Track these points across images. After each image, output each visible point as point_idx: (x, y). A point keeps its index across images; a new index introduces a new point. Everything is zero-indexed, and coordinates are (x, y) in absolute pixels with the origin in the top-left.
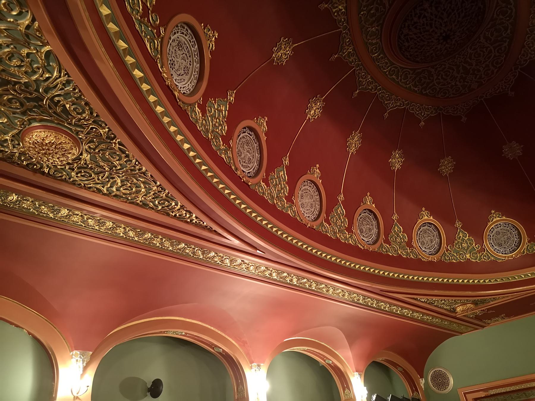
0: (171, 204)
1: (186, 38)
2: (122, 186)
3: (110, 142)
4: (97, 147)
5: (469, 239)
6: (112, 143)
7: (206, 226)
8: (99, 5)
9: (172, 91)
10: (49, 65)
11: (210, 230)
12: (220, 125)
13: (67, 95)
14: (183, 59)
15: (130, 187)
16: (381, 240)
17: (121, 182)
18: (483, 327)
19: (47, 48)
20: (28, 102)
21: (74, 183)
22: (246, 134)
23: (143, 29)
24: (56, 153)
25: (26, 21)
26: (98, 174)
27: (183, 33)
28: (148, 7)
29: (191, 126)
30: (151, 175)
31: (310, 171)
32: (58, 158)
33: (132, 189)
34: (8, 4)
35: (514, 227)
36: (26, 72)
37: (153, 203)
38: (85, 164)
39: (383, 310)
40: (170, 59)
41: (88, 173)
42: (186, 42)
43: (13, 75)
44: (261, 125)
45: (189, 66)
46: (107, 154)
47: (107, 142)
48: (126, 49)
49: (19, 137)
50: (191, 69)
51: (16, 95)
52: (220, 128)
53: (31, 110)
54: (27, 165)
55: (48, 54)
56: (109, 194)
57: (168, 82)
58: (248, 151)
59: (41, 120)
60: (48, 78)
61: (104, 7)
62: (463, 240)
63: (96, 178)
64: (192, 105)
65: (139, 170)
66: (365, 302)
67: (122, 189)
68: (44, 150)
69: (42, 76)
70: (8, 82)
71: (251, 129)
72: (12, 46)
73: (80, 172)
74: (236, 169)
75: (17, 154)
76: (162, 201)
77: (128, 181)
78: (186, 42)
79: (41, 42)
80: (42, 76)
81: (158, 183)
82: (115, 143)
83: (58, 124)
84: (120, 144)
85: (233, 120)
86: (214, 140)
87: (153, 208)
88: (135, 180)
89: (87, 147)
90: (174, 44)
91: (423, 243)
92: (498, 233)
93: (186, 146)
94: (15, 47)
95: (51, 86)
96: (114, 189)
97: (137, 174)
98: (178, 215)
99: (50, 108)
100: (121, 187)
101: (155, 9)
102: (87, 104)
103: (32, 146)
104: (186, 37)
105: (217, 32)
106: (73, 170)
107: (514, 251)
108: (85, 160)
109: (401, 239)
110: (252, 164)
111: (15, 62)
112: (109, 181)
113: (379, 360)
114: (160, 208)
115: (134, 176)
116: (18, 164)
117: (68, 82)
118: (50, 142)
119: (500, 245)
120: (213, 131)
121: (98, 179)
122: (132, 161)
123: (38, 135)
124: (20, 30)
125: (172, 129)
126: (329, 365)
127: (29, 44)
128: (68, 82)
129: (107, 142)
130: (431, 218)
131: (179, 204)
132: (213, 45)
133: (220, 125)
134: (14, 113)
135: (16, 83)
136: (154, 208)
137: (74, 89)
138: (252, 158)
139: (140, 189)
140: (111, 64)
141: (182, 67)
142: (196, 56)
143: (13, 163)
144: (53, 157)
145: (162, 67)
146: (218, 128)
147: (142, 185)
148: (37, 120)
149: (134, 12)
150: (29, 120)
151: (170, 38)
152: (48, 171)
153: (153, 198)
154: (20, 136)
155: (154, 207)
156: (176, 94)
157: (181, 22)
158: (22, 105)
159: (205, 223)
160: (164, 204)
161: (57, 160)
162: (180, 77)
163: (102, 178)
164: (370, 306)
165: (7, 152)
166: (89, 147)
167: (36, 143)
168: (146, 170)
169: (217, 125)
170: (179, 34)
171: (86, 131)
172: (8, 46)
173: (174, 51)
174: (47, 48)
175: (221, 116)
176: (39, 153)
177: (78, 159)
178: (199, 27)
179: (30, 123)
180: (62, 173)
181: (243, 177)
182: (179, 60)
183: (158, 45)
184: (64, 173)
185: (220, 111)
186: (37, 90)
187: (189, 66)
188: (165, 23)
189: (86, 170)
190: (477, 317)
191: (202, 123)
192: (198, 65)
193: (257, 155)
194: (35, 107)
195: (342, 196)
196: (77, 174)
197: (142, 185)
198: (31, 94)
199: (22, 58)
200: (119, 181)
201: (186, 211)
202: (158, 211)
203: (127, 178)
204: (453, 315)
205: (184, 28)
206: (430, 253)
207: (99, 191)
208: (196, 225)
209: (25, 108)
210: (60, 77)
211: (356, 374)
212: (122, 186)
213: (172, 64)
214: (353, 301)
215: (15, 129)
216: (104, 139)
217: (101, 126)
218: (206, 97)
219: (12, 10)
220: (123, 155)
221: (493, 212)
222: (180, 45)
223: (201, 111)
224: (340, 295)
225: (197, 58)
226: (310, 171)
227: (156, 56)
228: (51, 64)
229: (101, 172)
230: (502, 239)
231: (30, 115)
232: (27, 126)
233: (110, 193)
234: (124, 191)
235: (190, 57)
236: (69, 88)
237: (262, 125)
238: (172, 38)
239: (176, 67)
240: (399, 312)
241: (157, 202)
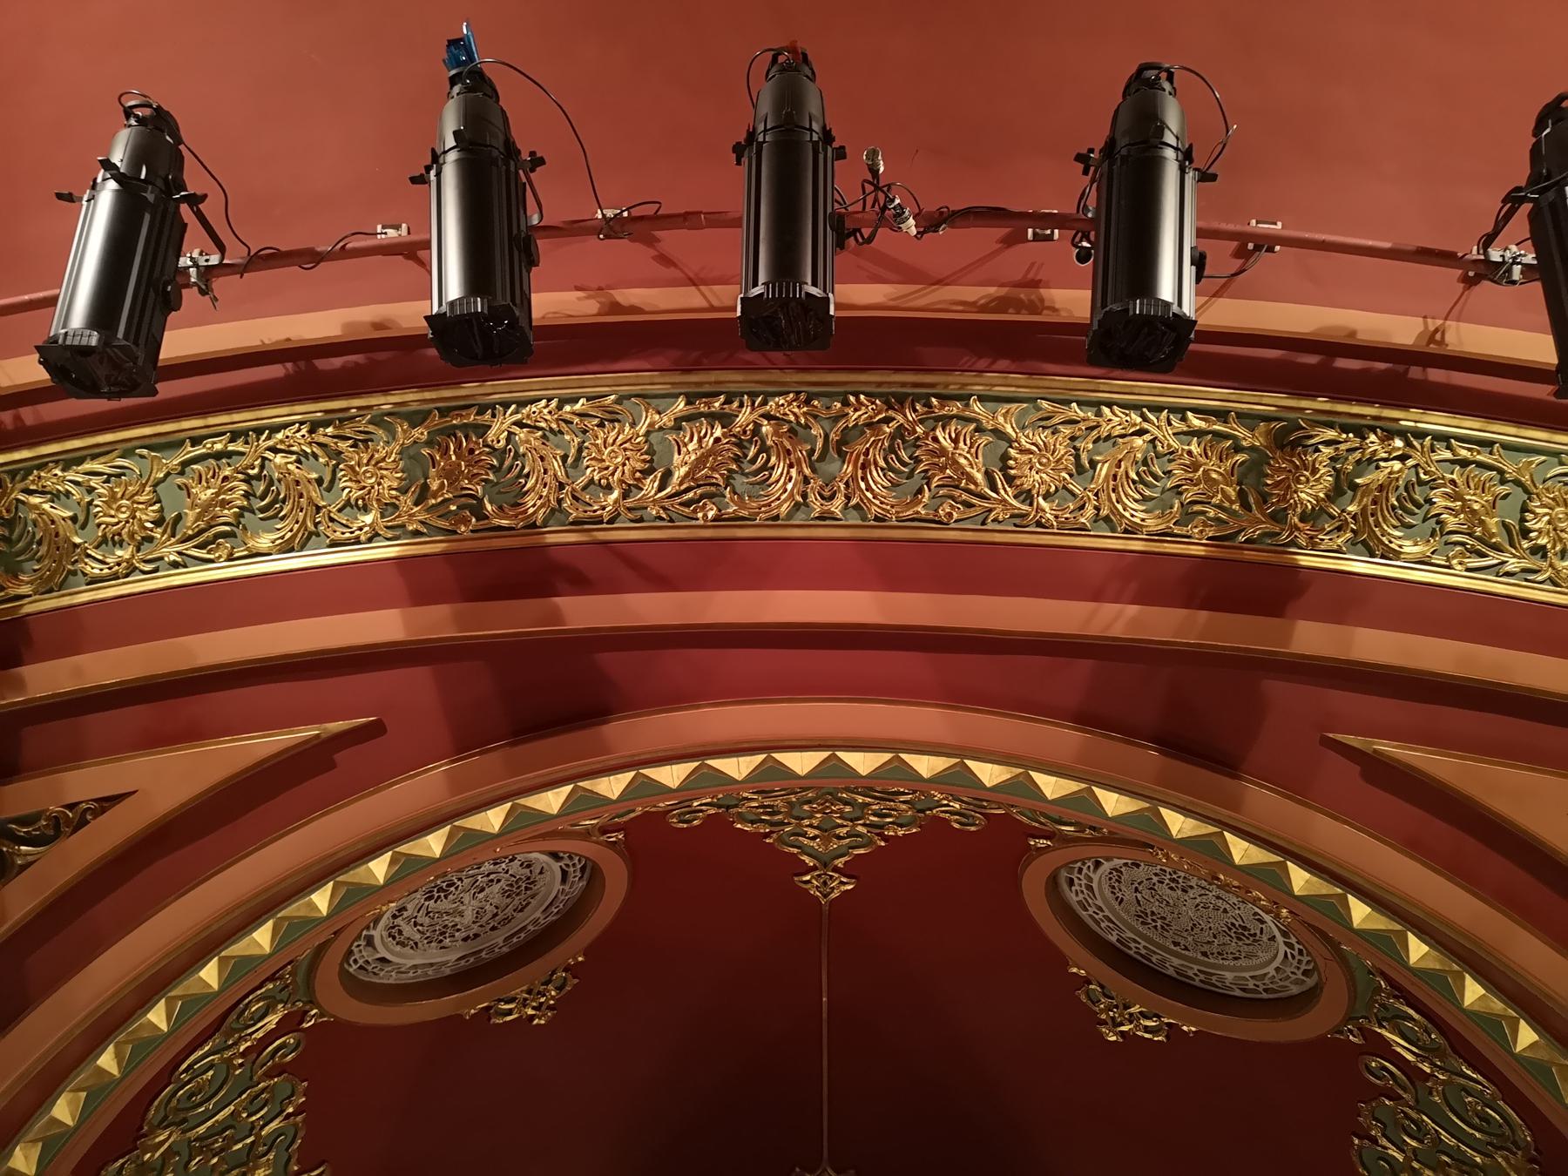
8: (31, 1136)
61: (36, 1151)
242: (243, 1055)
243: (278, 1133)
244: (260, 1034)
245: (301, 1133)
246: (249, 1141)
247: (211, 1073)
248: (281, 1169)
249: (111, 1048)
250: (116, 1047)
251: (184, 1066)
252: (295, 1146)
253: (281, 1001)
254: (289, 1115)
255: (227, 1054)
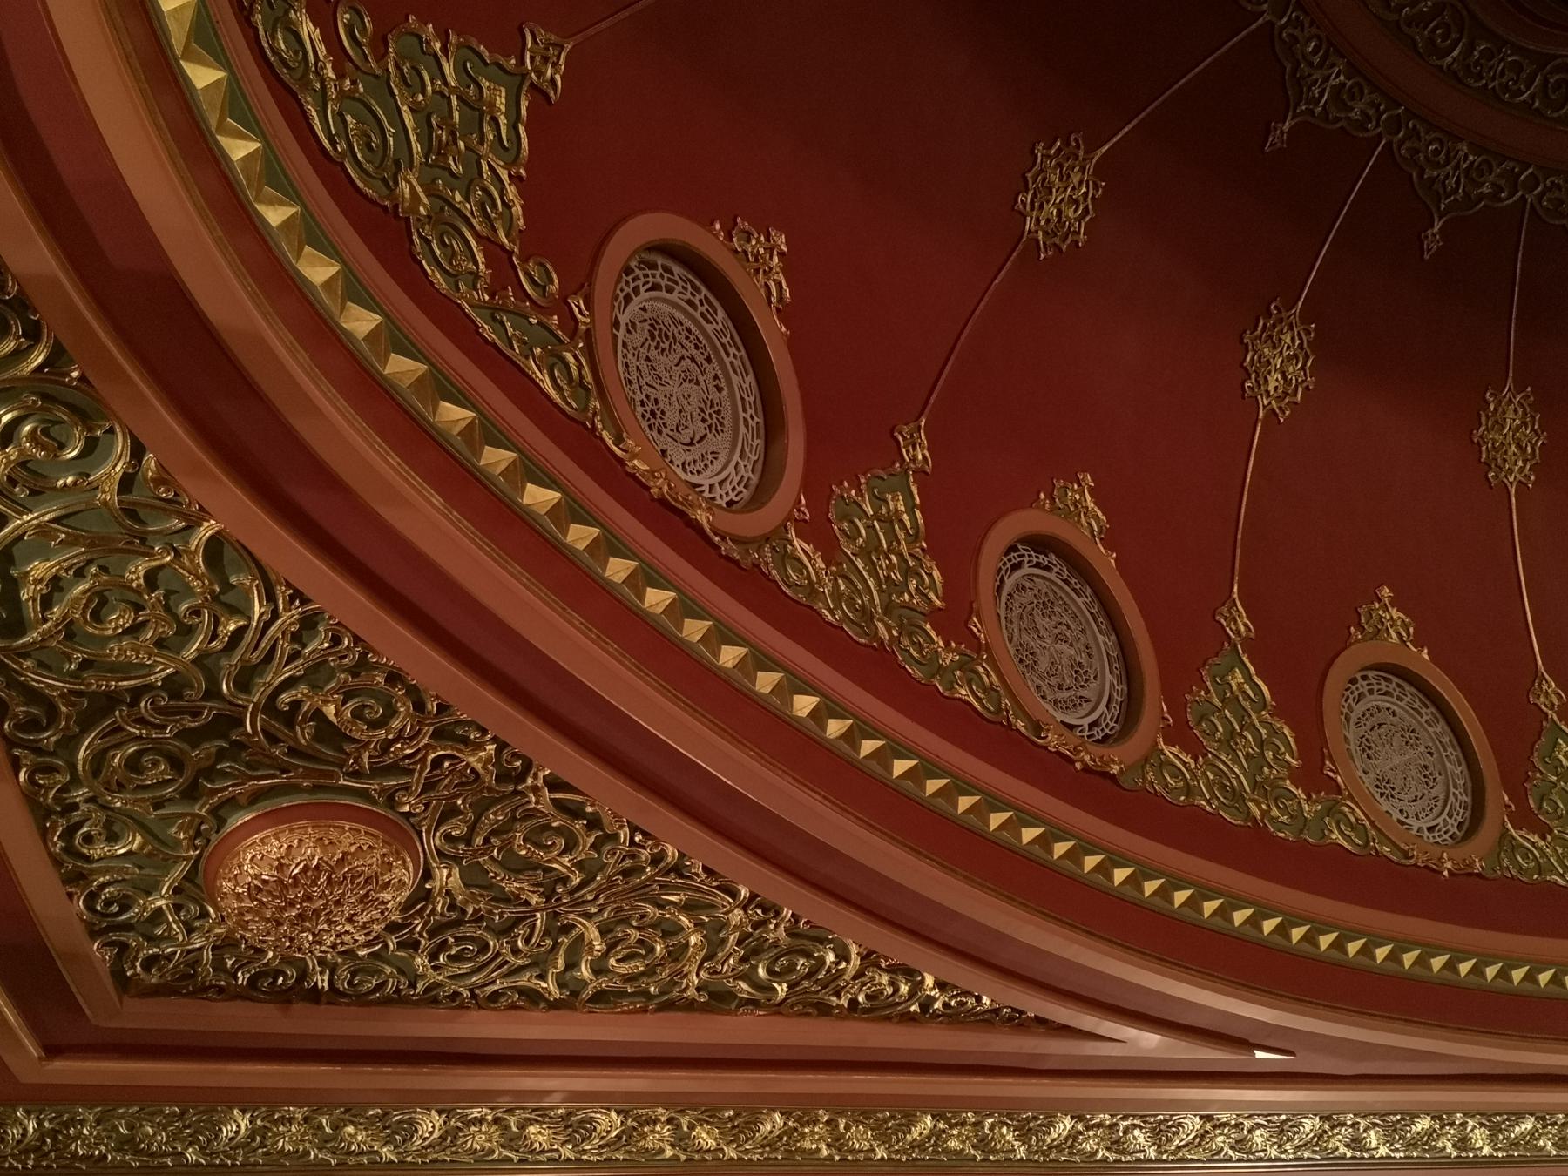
0: (822, 961)
1: (671, 300)
2: (611, 947)
3: (516, 793)
4: (473, 828)
6: (523, 794)
7: (996, 1011)
8: (335, 311)
9: (682, 515)
10: (227, 587)
11: (1019, 1022)
12: (908, 572)
13: (316, 674)
14: (686, 378)
15: (640, 942)
17: (604, 932)
19: (207, 530)
20: (194, 748)
21: (431, 998)
22: (1026, 570)
23: (510, 331)
24: (338, 903)
25: (115, 467)
26: (506, 931)
27: (655, 287)
28: (502, 247)
29: (797, 619)
30: (705, 869)
31: (1360, 626)
32: (350, 920)
33: (653, 950)
34: (45, 432)
36: (160, 643)
37: (749, 977)
38: (452, 907)
40: (640, 397)
41: (473, 939)
42: (678, 315)
43: (124, 670)
44: (1072, 514)
45: (715, 396)
46: (519, 841)
47: (504, 797)
48: (471, 425)
49: (196, 889)
50: (727, 403)
51: (148, 737)
52: (913, 584)
53: (210, 773)
54: (253, 981)
55: (214, 548)
56: (572, 999)
57: (659, 487)
58: (1058, 638)
59: (256, 797)
60: (239, 633)
61: (354, 309)
63: (507, 950)
64: (775, 536)
65: (656, 860)
67: (612, 961)
68: (291, 904)
69: (214, 637)
70: (111, 700)
71: (1040, 543)
72: (93, 570)
73: (444, 946)
74: (1037, 728)
75: (207, 955)
76: (783, 961)
77: (626, 921)
78: (678, 315)
79: (182, 516)
80: (214, 637)
81: (744, 892)
82: (535, 789)
83: (317, 788)
84: (554, 784)
85: (952, 539)
86: (905, 642)
87: (753, 1002)
88: (651, 910)
89: (438, 840)
90: (636, 339)
93: (804, 705)
94: (104, 569)
95: (256, 657)
96: (585, 972)
97: (651, 879)
98: (861, 998)
99: (273, 739)
100: (606, 955)
101: (535, 241)
102: (393, 678)
103: (247, 904)
104: (674, 297)
105: (780, 229)
106: (415, 945)
108: (448, 893)
110: (1094, 685)
111: (118, 619)
112: (556, 945)
114: (782, 990)
115: (642, 893)
116: (221, 990)
117: (309, 623)
118: (306, 868)
120: (888, 609)
121: (516, 952)
122: (615, 837)
123: (262, 853)
124: (105, 503)
125: (729, 656)
127: (143, 541)
128: (309, 623)
129: (504, 797)
131: (854, 949)
132: (779, 284)
133: (908, 572)
134: (158, 805)
135: (137, 693)
136: (762, 1001)
137: (336, 641)
138: (1084, 659)
139: (681, 938)
140: (437, 500)
141: (693, 408)
142: (732, 350)
143: (202, 991)
144: (330, 922)
145: (618, 440)
146: (902, 588)
147: (684, 921)
148: (243, 800)
149: (462, 285)
150: (214, 811)
151: (616, 324)
152: (331, 982)
153: (743, 960)
154: (200, 880)
155: (760, 996)
156: (702, 517)
157: (635, 252)
158: (176, 764)
159: (986, 1000)
160: (791, 968)
161: (350, 930)
162: (697, 451)
163: (527, 941)
165: (169, 958)
166: (448, 837)
167: (259, 889)
168: (682, 855)
169: (896, 576)
170: (644, 295)
171: (417, 781)
172: (80, 574)
173: (643, 364)
174: (207, 530)
175: (902, 535)
176: (279, 924)
177: (422, 896)
178: (708, 242)
179: (222, 822)
180: (380, 972)
181: (1075, 751)
182: (673, 388)
183: (580, 367)
184: (388, 970)
185: (889, 521)
186: (213, 693)
187: (715, 396)
188: (581, 282)
189: (462, 931)
191: (837, 595)
192: (751, 378)
193: (1105, 641)
194: (221, 755)
195: (1550, 685)
196: (433, 956)
197: (684, 921)
198: (196, 713)
199: (133, 597)
200: (593, 933)
201: (891, 970)
202: (778, 1009)
203: (618, 910)
205: (653, 266)
207: (533, 997)
208: (954, 1018)
209: (189, 773)
210: (275, 615)
212: (611, 947)
213: (653, 414)
215: (177, 860)
216: (490, 789)
217: (465, 741)
218: (816, 486)
219: (62, 446)
220: (579, 825)
222: (657, 332)
223: (817, 548)
225: (736, 356)
226: (1360, 626)
227: (586, 409)
228: (233, 580)
229: (518, 921)
231: (214, 792)
232: (214, 838)
233: (575, 994)
234: (624, 969)
235: (709, 360)
236: (318, 644)
237: (1080, 514)
238: (624, 319)
239: (672, 417)
241: (761, 971)
242: (341, 76)
243: (460, 69)
244: (322, 50)
245: (474, 43)
246: (455, 102)
247: (349, 118)
248: (506, 77)
249: (260, 208)
250: (260, 202)
251: (326, 143)
252: (486, 54)
253: (287, 12)
254: (445, 50)
255: (333, 94)
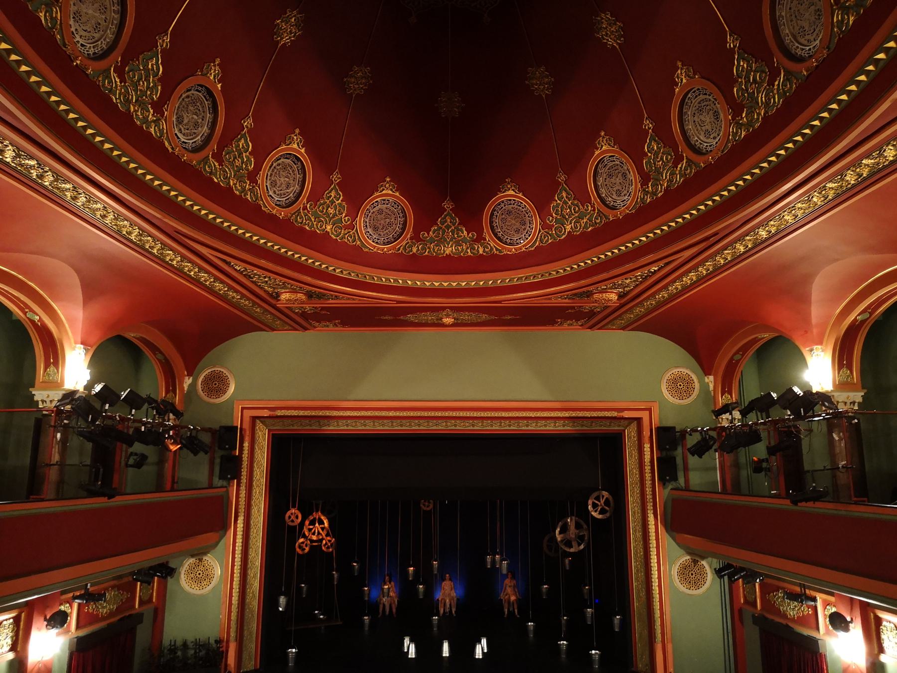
5: (340, 205)
16: (209, 152)
18: (306, 329)
35: (403, 211)
39: (167, 263)
62: (333, 202)
66: (140, 240)
91: (274, 184)
92: (380, 212)
107: (389, 243)
109: (243, 162)
113: (131, 335)
119: (375, 229)
126: (33, 322)
130: (303, 151)
164: (147, 250)
190: (304, 315)
204: (273, 302)
206: (278, 203)
211: (80, 349)
214: (119, 232)
221: (388, 179)
224: (98, 213)
230: (382, 222)
240: (192, 273)
